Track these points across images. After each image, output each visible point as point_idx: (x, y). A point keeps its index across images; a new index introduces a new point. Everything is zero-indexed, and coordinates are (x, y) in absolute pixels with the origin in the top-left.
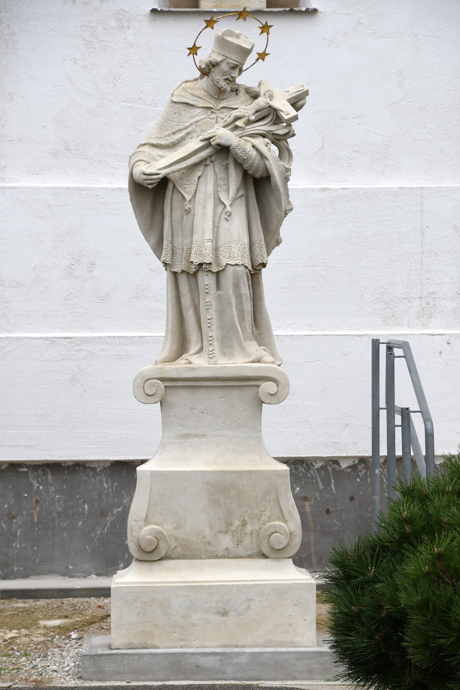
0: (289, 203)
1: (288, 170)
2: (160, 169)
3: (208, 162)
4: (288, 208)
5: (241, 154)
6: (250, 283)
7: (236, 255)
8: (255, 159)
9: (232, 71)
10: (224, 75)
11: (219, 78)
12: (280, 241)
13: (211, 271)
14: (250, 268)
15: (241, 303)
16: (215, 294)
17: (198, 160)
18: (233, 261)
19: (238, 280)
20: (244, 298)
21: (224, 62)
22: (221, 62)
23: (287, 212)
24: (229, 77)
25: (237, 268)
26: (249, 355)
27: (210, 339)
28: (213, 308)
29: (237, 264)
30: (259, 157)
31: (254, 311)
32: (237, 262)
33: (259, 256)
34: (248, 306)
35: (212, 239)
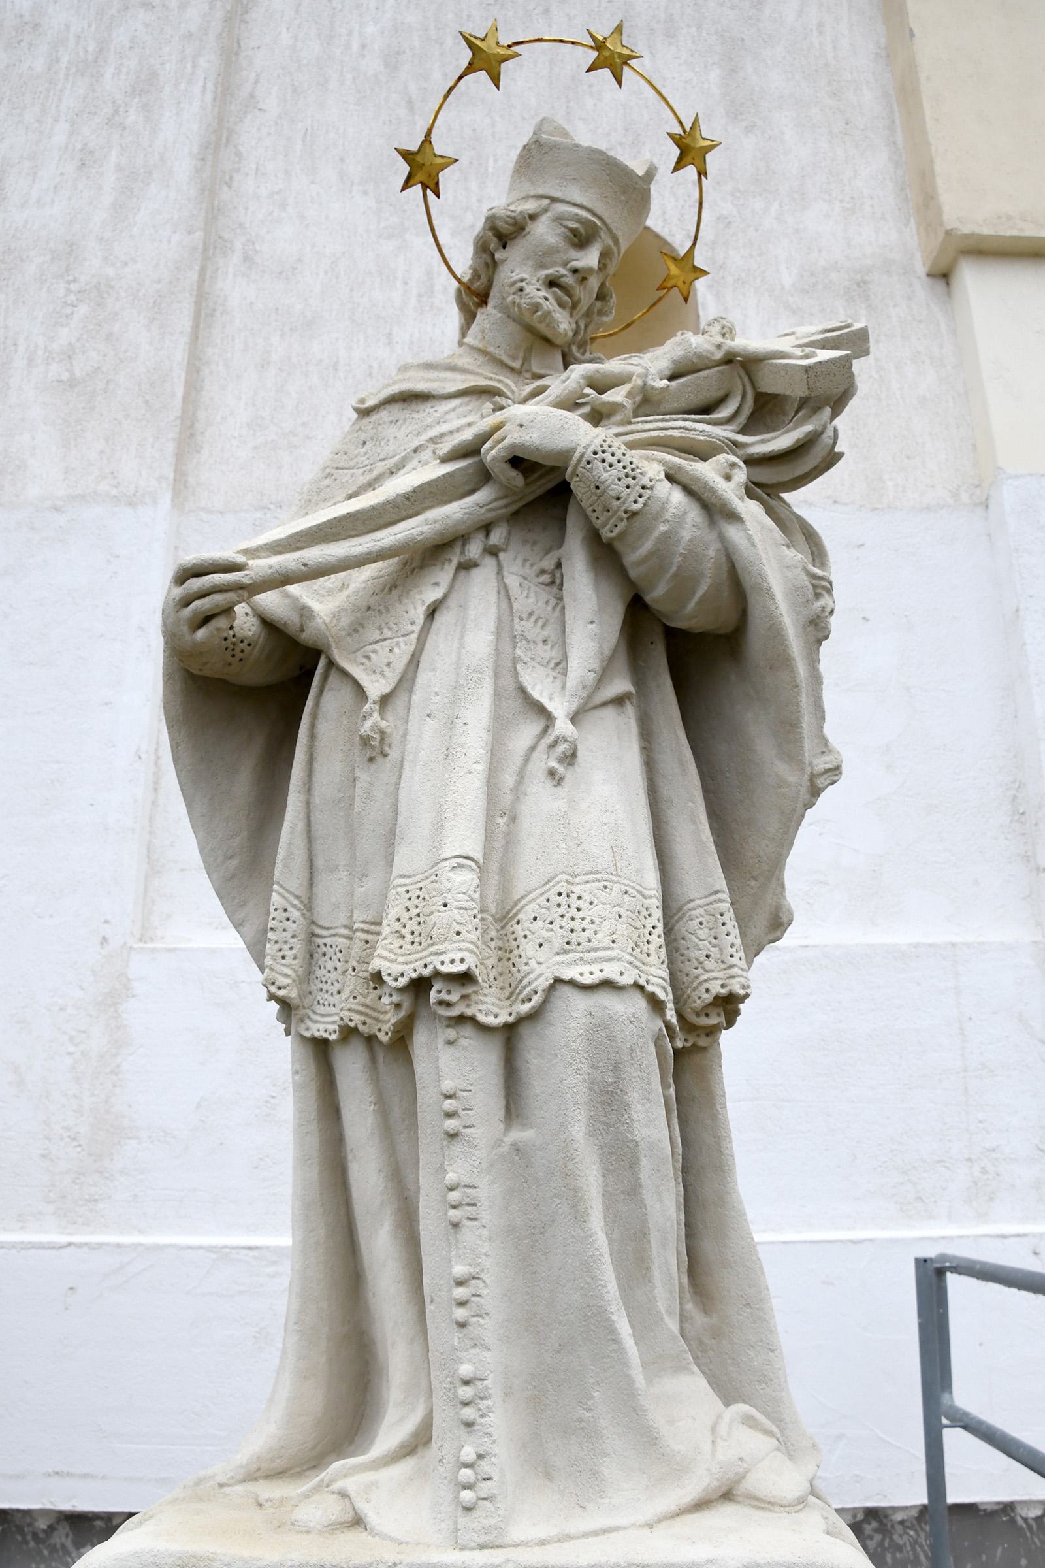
0: (824, 745)
1: (821, 587)
2: (252, 553)
3: (474, 549)
4: (821, 764)
5: (618, 488)
6: (672, 1091)
7: (602, 939)
8: (680, 518)
9: (573, 253)
10: (543, 266)
11: (525, 276)
12: (785, 919)
13: (473, 1020)
15: (634, 1191)
16: (498, 1143)
17: (425, 528)
18: (586, 969)
19: (616, 1068)
20: (644, 1162)
21: (544, 218)
22: (533, 217)
23: (820, 782)
24: (563, 271)
25: (608, 1001)
26: (677, 1468)
27: (466, 1392)
28: (486, 1216)
29: (607, 985)
30: (694, 515)
31: (687, 1225)
32: (611, 971)
33: (709, 964)
34: (664, 1206)
35: (478, 856)
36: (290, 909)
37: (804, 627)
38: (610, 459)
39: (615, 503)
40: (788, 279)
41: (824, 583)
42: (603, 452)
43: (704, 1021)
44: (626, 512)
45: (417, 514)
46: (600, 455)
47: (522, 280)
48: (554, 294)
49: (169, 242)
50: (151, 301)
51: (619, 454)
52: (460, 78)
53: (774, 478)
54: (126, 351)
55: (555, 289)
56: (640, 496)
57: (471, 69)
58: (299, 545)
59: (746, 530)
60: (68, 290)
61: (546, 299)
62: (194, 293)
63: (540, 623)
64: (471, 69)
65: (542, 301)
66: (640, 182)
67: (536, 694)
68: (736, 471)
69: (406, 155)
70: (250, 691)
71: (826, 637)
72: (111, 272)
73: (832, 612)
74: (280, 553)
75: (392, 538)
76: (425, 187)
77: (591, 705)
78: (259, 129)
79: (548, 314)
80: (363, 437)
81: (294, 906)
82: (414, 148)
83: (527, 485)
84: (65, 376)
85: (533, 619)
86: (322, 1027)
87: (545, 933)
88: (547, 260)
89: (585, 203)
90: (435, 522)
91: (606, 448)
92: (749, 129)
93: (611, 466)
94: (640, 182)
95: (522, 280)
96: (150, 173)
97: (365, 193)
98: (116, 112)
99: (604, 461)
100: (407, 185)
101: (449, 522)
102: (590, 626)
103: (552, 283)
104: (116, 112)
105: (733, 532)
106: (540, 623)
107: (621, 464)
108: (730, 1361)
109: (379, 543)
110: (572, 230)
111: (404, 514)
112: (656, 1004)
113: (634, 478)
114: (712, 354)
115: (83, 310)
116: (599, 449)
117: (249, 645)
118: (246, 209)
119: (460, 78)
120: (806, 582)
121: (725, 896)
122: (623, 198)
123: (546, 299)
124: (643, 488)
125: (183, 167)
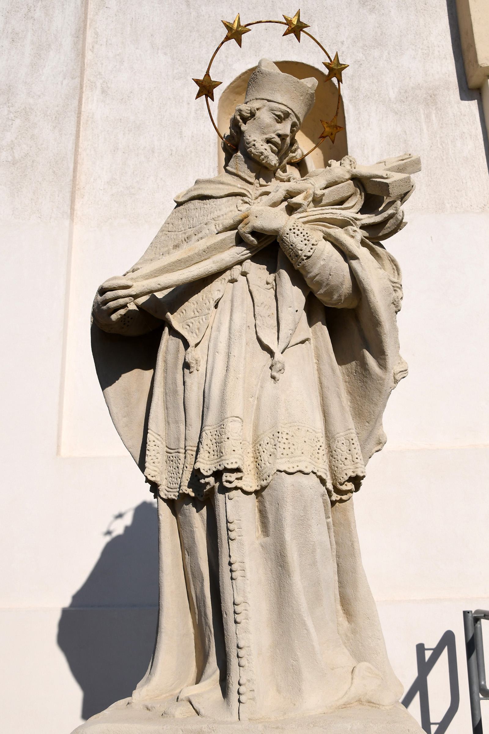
1: (397, 287)
4: (397, 369)
9: (279, 126)
10: (264, 133)
11: (255, 139)
12: (383, 441)
14: (330, 486)
15: (314, 563)
18: (291, 466)
20: (318, 551)
22: (258, 109)
23: (398, 377)
24: (274, 135)
31: (340, 582)
36: (156, 441)
37: (389, 306)
38: (297, 232)
39: (300, 252)
40: (393, 94)
41: (397, 285)
42: (294, 229)
43: (344, 488)
44: (305, 256)
45: (209, 258)
46: (293, 231)
47: (254, 141)
48: (270, 146)
49: (62, 84)
50: (54, 117)
51: (301, 230)
52: (222, 43)
53: (375, 235)
54: (42, 144)
55: (269, 144)
56: (311, 249)
57: (227, 38)
58: (156, 275)
59: (360, 263)
60: (10, 112)
61: (266, 149)
62: (77, 112)
63: (267, 307)
64: (227, 38)
65: (264, 151)
66: (310, 90)
67: (266, 341)
68: (356, 234)
69: (197, 81)
70: (128, 337)
71: (399, 310)
72: (31, 101)
73: (402, 298)
74: (147, 279)
75: (198, 270)
76: (207, 96)
77: (293, 342)
78: (107, 19)
79: (267, 157)
80: (180, 216)
81: (158, 439)
82: (201, 78)
83: (259, 243)
84: (10, 158)
85: (263, 305)
86: (172, 494)
87: (272, 450)
88: (266, 131)
89: (283, 103)
90: (218, 262)
91: (295, 227)
92: (372, 10)
93: (298, 235)
94: (310, 90)
95: (254, 141)
96: (49, 45)
97: (165, 54)
98: (29, 10)
99: (294, 233)
100: (198, 96)
101: (224, 262)
102: (290, 309)
103: (268, 141)
104: (29, 10)
105: (354, 263)
106: (267, 307)
107: (302, 234)
108: (360, 644)
109: (192, 273)
110: (277, 115)
111: (203, 258)
112: (323, 481)
113: (308, 240)
114: (345, 176)
115: (18, 122)
116: (292, 228)
117: (132, 318)
118: (102, 64)
119: (222, 43)
120: (390, 284)
121: (354, 431)
122: (301, 98)
123: (266, 149)
124: (313, 245)
125: (67, 42)
